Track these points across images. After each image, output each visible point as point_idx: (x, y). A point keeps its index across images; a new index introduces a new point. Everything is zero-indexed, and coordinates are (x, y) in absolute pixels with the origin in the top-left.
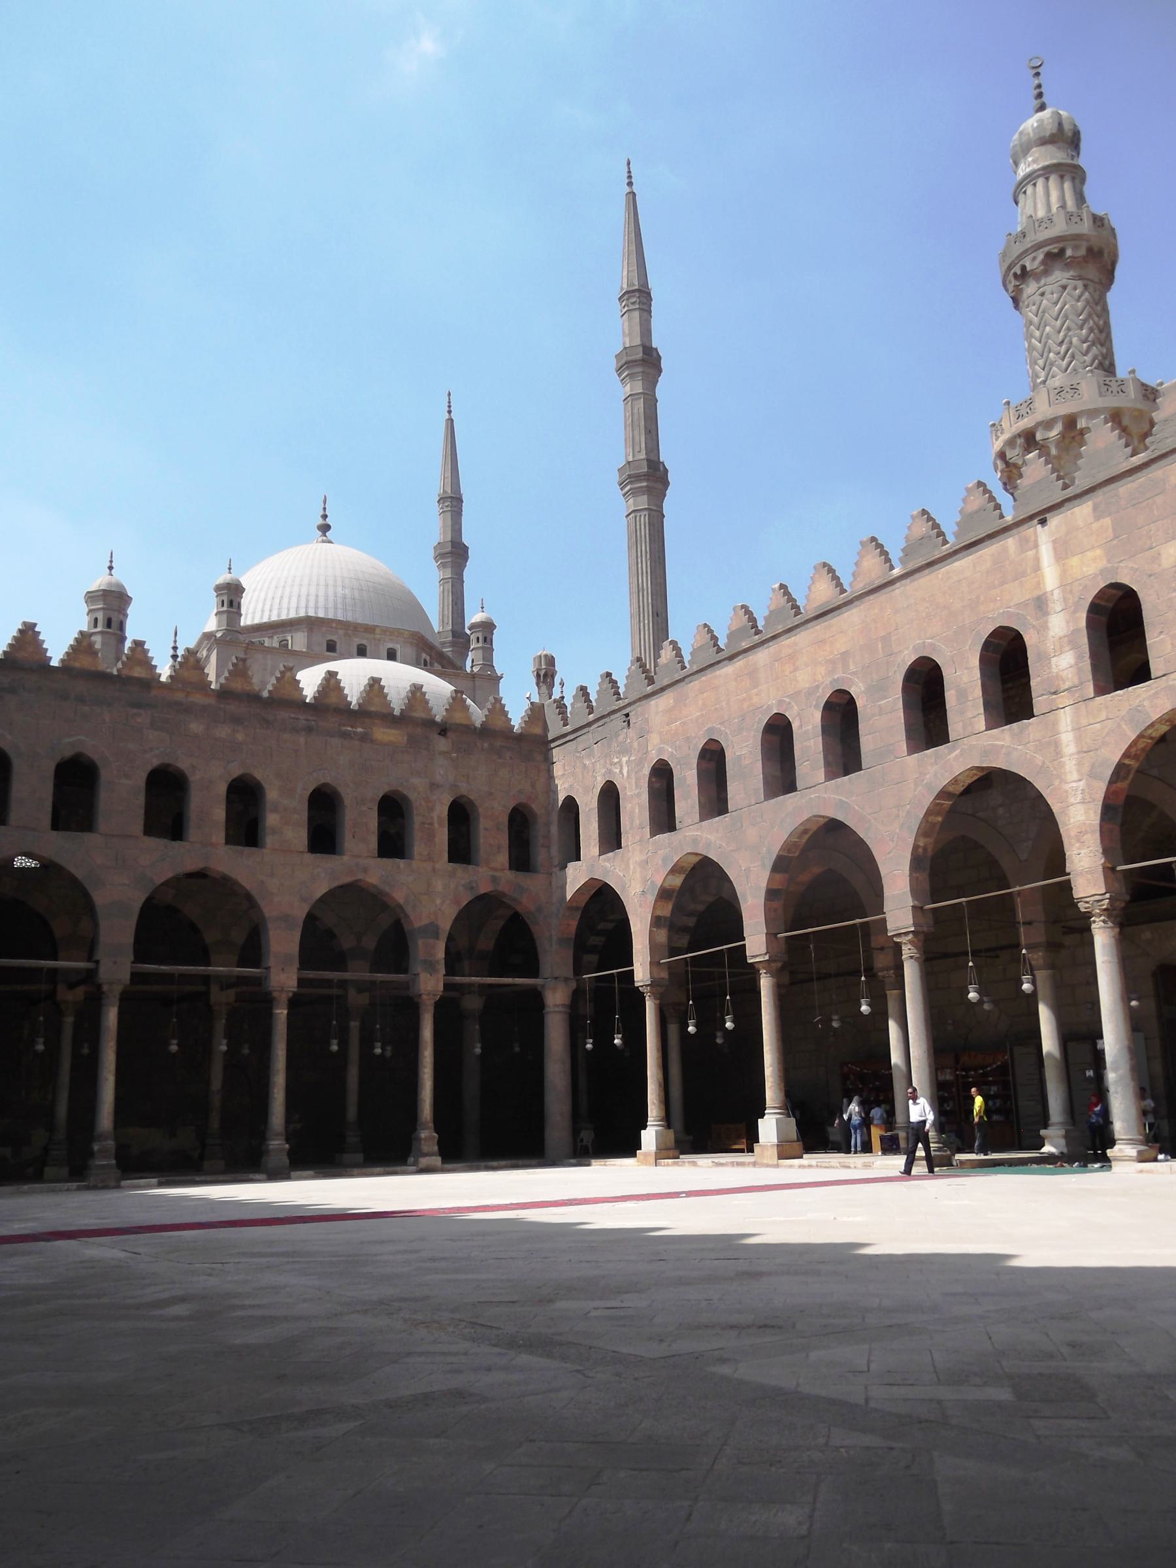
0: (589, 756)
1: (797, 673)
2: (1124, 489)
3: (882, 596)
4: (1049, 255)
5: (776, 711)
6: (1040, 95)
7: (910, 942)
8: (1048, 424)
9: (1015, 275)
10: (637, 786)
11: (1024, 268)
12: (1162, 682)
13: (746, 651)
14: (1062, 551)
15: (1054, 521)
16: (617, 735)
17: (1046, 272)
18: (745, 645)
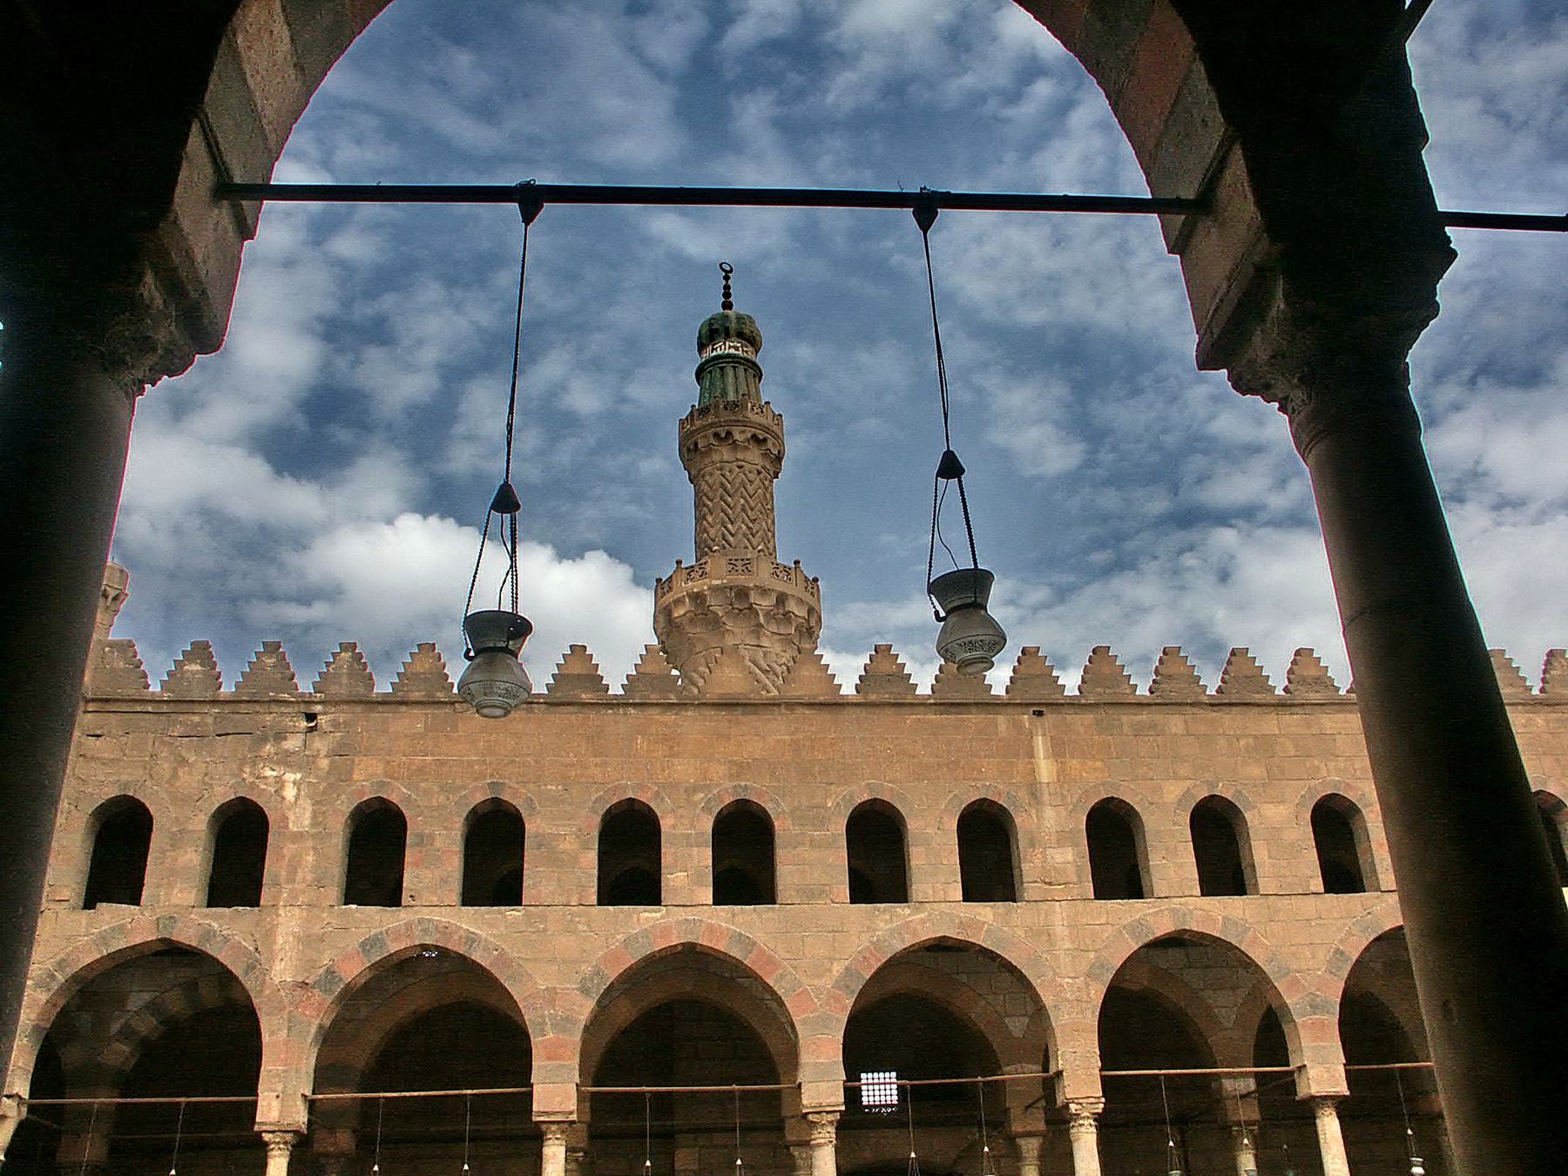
0: (198, 752)
1: (676, 761)
2: (1128, 719)
3: (825, 716)
4: (754, 436)
5: (631, 795)
6: (727, 295)
7: (831, 1122)
8: (764, 592)
9: (716, 435)
10: (314, 824)
11: (729, 434)
12: (1165, 904)
13: (584, 704)
14: (1058, 751)
15: (1050, 717)
16: (280, 736)
17: (747, 448)
18: (586, 697)
